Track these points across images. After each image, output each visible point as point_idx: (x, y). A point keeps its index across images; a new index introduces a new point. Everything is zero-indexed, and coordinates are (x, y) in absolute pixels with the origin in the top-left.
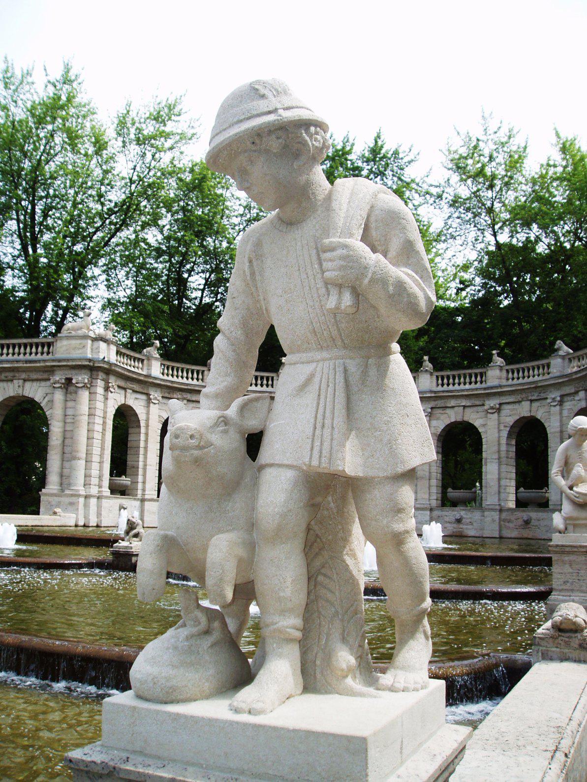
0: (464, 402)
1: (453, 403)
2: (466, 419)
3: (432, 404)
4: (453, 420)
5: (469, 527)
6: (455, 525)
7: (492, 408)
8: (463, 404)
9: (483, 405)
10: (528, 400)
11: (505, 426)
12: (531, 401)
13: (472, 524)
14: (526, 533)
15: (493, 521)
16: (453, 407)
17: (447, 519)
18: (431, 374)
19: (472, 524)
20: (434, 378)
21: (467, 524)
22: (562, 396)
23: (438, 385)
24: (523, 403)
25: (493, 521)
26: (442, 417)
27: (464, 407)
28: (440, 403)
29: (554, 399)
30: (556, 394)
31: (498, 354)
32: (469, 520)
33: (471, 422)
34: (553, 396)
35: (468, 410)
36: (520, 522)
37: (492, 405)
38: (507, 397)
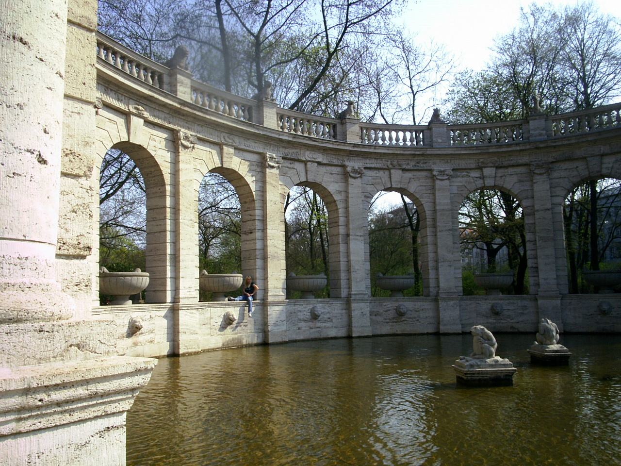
0: (320, 158)
1: (307, 155)
3: (283, 151)
5: (328, 325)
6: (311, 324)
7: (355, 171)
8: (319, 160)
10: (400, 169)
12: (404, 170)
13: (332, 321)
14: (399, 328)
15: (363, 314)
16: (305, 162)
17: (301, 316)
19: (332, 321)
21: (325, 321)
25: (363, 314)
27: (319, 163)
28: (291, 152)
29: (442, 172)
30: (447, 167)
32: (328, 316)
33: (324, 185)
34: (442, 169)
35: (323, 169)
36: (392, 314)
37: (356, 168)
38: (373, 161)
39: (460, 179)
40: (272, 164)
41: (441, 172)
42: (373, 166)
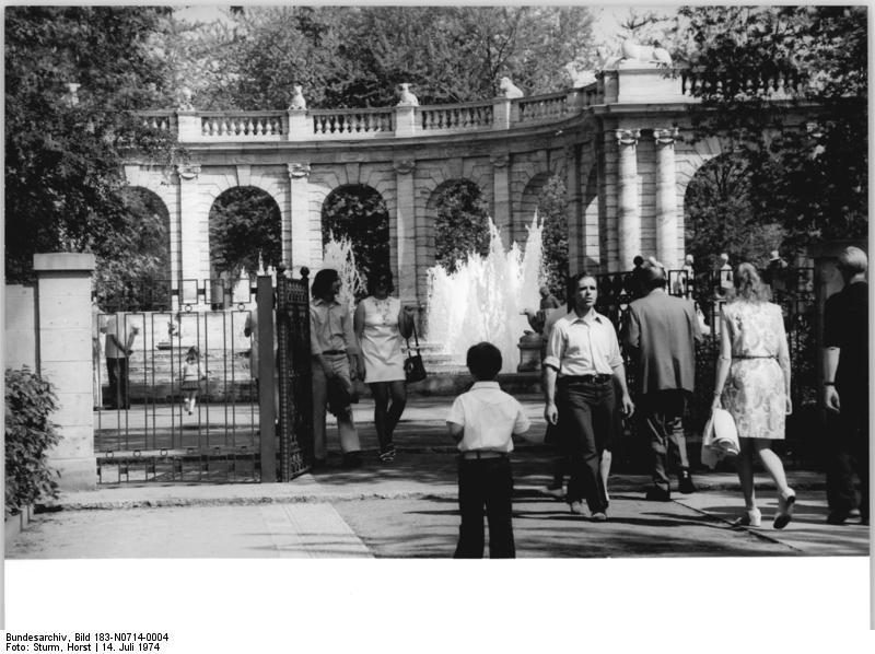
2: (363, 181)
4: (343, 182)
7: (403, 166)
8: (360, 160)
9: (391, 162)
11: (423, 193)
16: (344, 164)
18: (307, 114)
20: (312, 121)
22: (511, 155)
23: (316, 130)
24: (451, 161)
26: (327, 178)
27: (361, 164)
28: (324, 158)
29: (499, 158)
31: (409, 88)
35: (367, 170)
37: (404, 162)
39: (520, 165)
40: (297, 174)
41: (499, 158)
42: (427, 157)
